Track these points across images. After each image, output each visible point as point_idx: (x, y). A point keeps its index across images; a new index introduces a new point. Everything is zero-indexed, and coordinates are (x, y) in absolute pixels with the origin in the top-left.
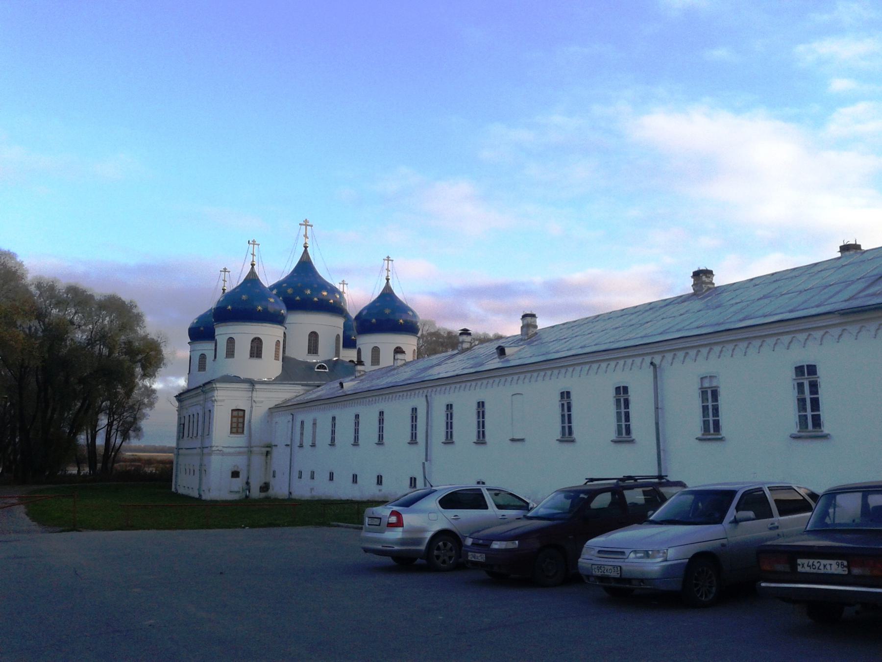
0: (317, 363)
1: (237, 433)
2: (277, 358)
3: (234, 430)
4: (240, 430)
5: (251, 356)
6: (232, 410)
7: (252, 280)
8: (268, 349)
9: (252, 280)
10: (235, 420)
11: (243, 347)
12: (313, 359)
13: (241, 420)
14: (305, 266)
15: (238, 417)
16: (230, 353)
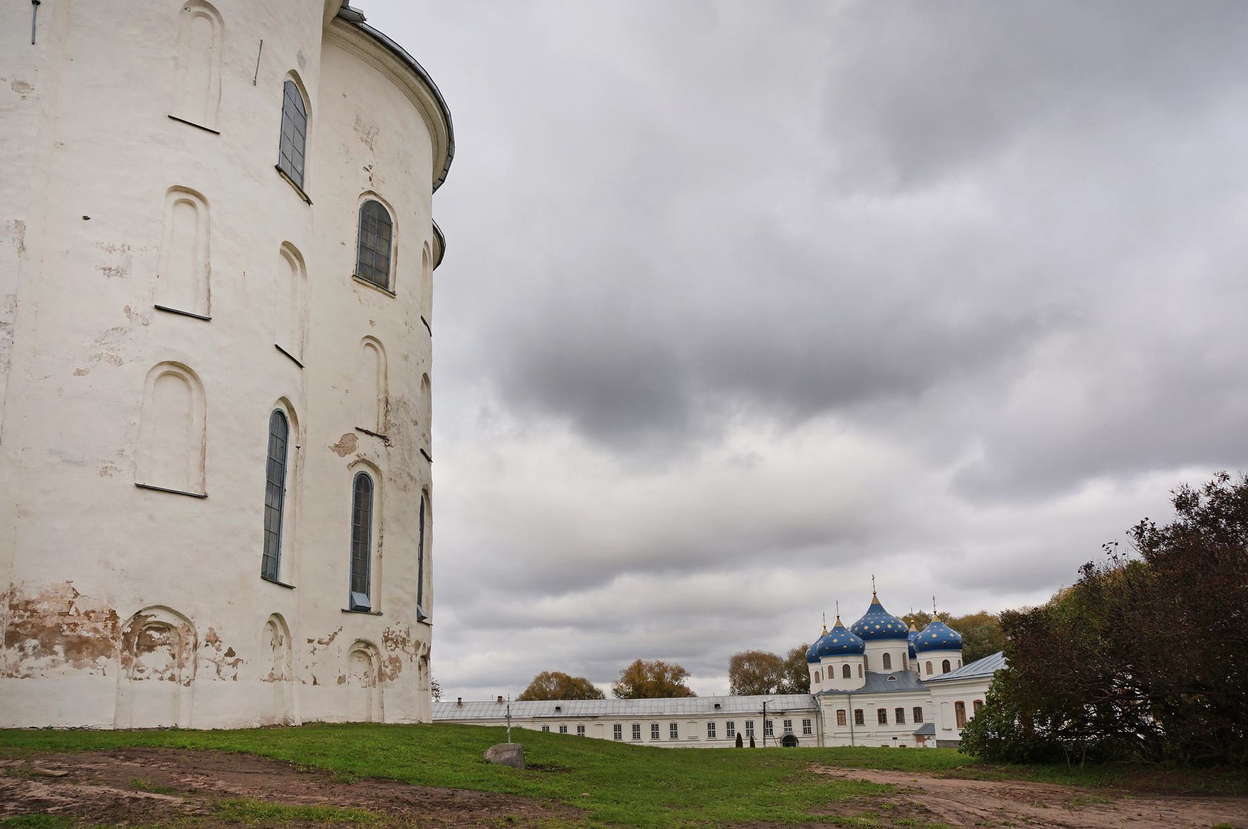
0: (889, 675)
1: (842, 724)
2: (860, 676)
3: (840, 723)
4: (843, 723)
5: (844, 677)
6: (838, 711)
7: (839, 628)
8: (854, 671)
9: (839, 628)
10: (840, 716)
11: (839, 671)
12: (889, 672)
13: (843, 716)
14: (876, 608)
15: (841, 715)
16: (831, 675)
